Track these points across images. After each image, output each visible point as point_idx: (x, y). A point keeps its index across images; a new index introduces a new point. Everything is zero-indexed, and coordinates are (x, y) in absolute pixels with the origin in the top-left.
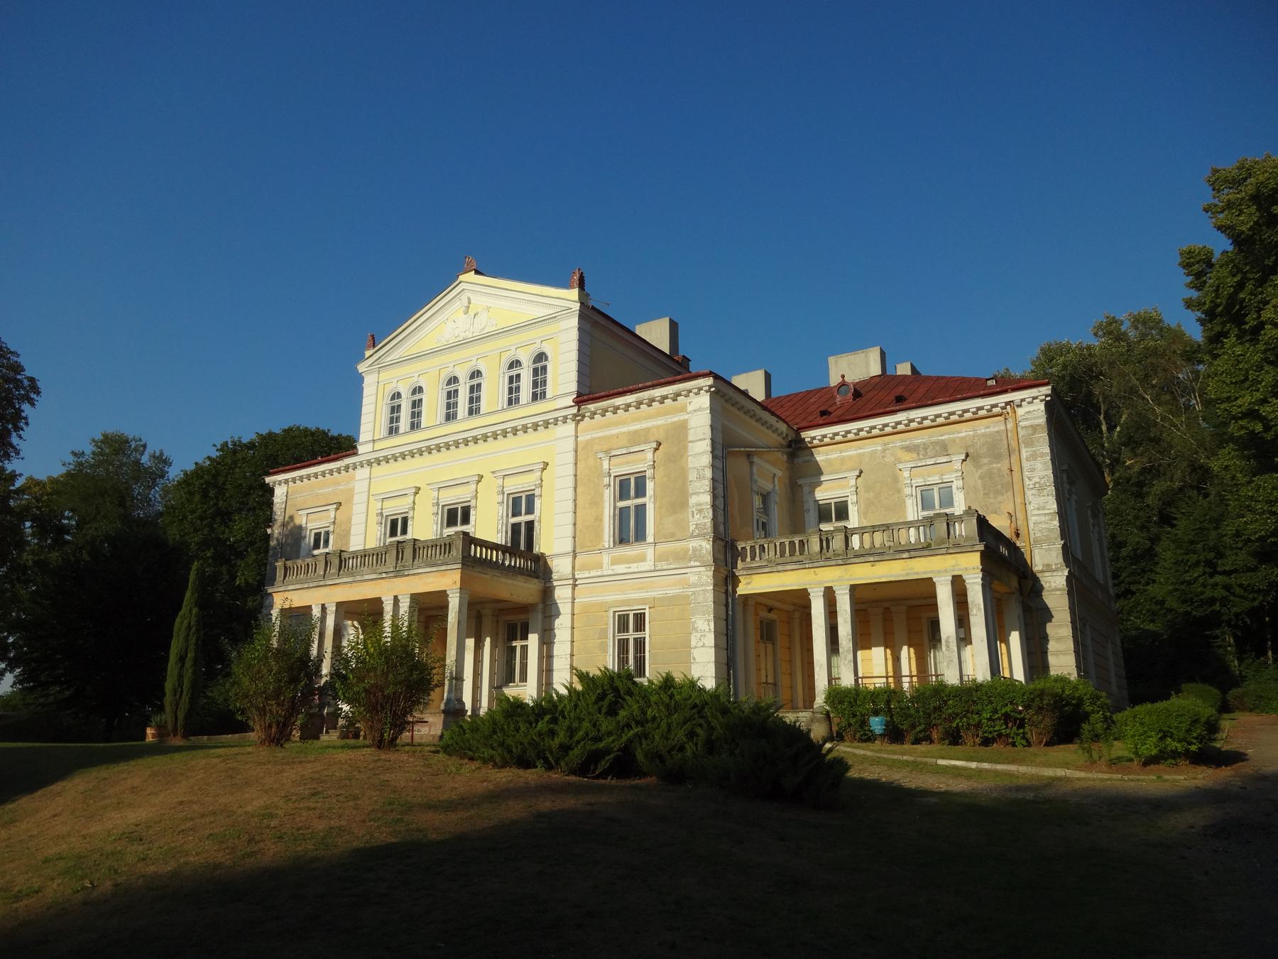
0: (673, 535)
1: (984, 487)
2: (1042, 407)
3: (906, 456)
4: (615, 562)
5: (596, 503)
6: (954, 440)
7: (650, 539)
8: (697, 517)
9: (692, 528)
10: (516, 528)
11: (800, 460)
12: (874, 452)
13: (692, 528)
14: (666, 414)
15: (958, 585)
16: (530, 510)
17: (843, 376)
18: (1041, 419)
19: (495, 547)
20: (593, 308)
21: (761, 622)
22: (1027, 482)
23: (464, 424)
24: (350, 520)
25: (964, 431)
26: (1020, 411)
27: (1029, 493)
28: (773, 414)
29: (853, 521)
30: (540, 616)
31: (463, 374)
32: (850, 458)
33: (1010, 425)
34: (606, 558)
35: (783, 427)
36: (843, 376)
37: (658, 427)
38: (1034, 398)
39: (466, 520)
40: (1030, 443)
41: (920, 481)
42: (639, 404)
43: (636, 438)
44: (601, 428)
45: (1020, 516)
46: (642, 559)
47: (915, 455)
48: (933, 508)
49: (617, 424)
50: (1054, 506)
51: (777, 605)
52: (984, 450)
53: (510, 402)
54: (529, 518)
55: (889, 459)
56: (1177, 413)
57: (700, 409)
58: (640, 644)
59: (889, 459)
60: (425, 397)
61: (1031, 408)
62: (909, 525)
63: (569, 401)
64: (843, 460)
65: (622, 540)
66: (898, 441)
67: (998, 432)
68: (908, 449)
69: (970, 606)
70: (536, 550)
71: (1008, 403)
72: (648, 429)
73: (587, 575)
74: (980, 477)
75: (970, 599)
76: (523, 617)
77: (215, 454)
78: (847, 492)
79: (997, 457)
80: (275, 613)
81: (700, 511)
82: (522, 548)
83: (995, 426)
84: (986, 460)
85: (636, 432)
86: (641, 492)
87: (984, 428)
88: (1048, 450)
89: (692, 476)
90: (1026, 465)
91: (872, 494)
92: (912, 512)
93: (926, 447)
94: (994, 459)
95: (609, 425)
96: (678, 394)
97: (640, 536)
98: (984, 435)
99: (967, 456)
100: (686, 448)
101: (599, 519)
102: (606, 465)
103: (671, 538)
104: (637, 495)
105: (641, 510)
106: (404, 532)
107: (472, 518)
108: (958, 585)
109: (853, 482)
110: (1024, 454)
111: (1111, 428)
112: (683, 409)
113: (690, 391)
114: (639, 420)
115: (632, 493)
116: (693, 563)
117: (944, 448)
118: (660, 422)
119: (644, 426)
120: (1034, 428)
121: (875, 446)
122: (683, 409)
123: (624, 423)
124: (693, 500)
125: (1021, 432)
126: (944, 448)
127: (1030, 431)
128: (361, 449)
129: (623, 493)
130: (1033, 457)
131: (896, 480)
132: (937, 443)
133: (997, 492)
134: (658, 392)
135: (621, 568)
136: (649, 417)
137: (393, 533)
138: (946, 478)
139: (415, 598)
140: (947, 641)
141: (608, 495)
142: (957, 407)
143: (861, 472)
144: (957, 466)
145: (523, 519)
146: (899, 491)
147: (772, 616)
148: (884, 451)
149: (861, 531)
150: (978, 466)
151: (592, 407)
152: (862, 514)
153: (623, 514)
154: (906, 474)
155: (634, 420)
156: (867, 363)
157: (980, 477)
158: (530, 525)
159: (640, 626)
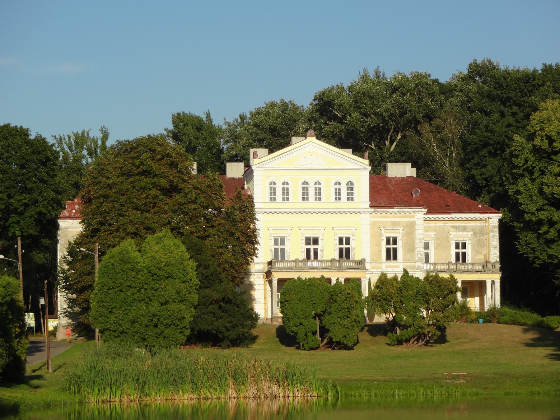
0: (409, 260)
2: (498, 220)
4: (387, 267)
5: (379, 245)
6: (468, 226)
9: (417, 259)
10: (341, 250)
12: (441, 226)
13: (417, 259)
14: (407, 217)
15: (493, 282)
16: (348, 242)
18: (497, 224)
23: (312, 203)
25: (472, 224)
26: (491, 220)
32: (432, 227)
33: (487, 224)
37: (403, 221)
40: (493, 232)
43: (394, 224)
44: (379, 217)
45: (487, 255)
46: (399, 267)
49: (387, 217)
50: (498, 254)
52: (478, 232)
54: (347, 246)
56: (445, 156)
57: (420, 218)
59: (446, 229)
60: (290, 187)
61: (494, 220)
63: (367, 205)
65: (388, 258)
66: (449, 224)
68: (453, 227)
72: (399, 222)
73: (375, 270)
74: (477, 241)
78: (430, 239)
80: (58, 257)
81: (420, 254)
83: (482, 224)
84: (478, 235)
85: (394, 222)
87: (479, 224)
88: (498, 235)
89: (417, 241)
90: (491, 239)
93: (459, 227)
94: (480, 234)
95: (383, 217)
97: (395, 258)
101: (380, 251)
102: (383, 232)
103: (408, 261)
105: (395, 250)
108: (493, 282)
109: (433, 236)
111: (392, 142)
114: (396, 217)
117: (465, 229)
120: (495, 227)
121: (441, 224)
122: (413, 217)
123: (390, 217)
124: (417, 250)
129: (388, 242)
130: (494, 236)
131: (448, 237)
133: (481, 247)
134: (406, 210)
136: (399, 217)
138: (465, 239)
142: (472, 215)
144: (470, 236)
145: (344, 246)
146: (449, 241)
150: (476, 237)
151: (379, 210)
152: (436, 248)
153: (388, 250)
155: (394, 217)
156: (405, 169)
157: (477, 241)
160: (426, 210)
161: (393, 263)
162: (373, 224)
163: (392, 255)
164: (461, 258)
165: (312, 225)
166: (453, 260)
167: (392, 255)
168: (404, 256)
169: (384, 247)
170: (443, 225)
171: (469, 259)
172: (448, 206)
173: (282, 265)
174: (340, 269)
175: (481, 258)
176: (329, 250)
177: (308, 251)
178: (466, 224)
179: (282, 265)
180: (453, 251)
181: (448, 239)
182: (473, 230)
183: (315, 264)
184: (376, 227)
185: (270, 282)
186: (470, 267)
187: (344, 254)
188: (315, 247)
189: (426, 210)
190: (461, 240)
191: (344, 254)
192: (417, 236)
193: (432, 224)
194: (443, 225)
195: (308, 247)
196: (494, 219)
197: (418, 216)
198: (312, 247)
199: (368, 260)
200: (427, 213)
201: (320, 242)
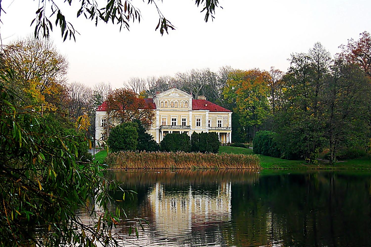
3: (217, 117)
25: (223, 115)
31: (174, 102)
65: (197, 125)
83: (226, 115)
86: (200, 121)
89: (206, 120)
97: (199, 125)
105: (200, 123)
112: (206, 113)
121: (214, 115)
124: (206, 123)
126: (221, 116)
139: (184, 132)
141: (196, 120)
153: (197, 123)
160: (209, 111)
161: (198, 127)
162: (192, 114)
163: (198, 124)
164: (220, 126)
165: (174, 115)
166: (217, 126)
167: (198, 124)
169: (196, 122)
171: (222, 126)
172: (216, 109)
173: (165, 127)
174: (183, 129)
175: (226, 126)
176: (179, 123)
177: (173, 123)
178: (221, 115)
179: (165, 127)
180: (217, 123)
181: (216, 120)
183: (175, 127)
184: (194, 116)
186: (222, 129)
187: (184, 124)
188: (175, 121)
189: (209, 111)
190: (220, 120)
191: (184, 124)
193: (211, 115)
195: (173, 121)
196: (230, 113)
197: (207, 112)
198: (174, 121)
199: (191, 126)
200: (210, 111)
201: (176, 120)
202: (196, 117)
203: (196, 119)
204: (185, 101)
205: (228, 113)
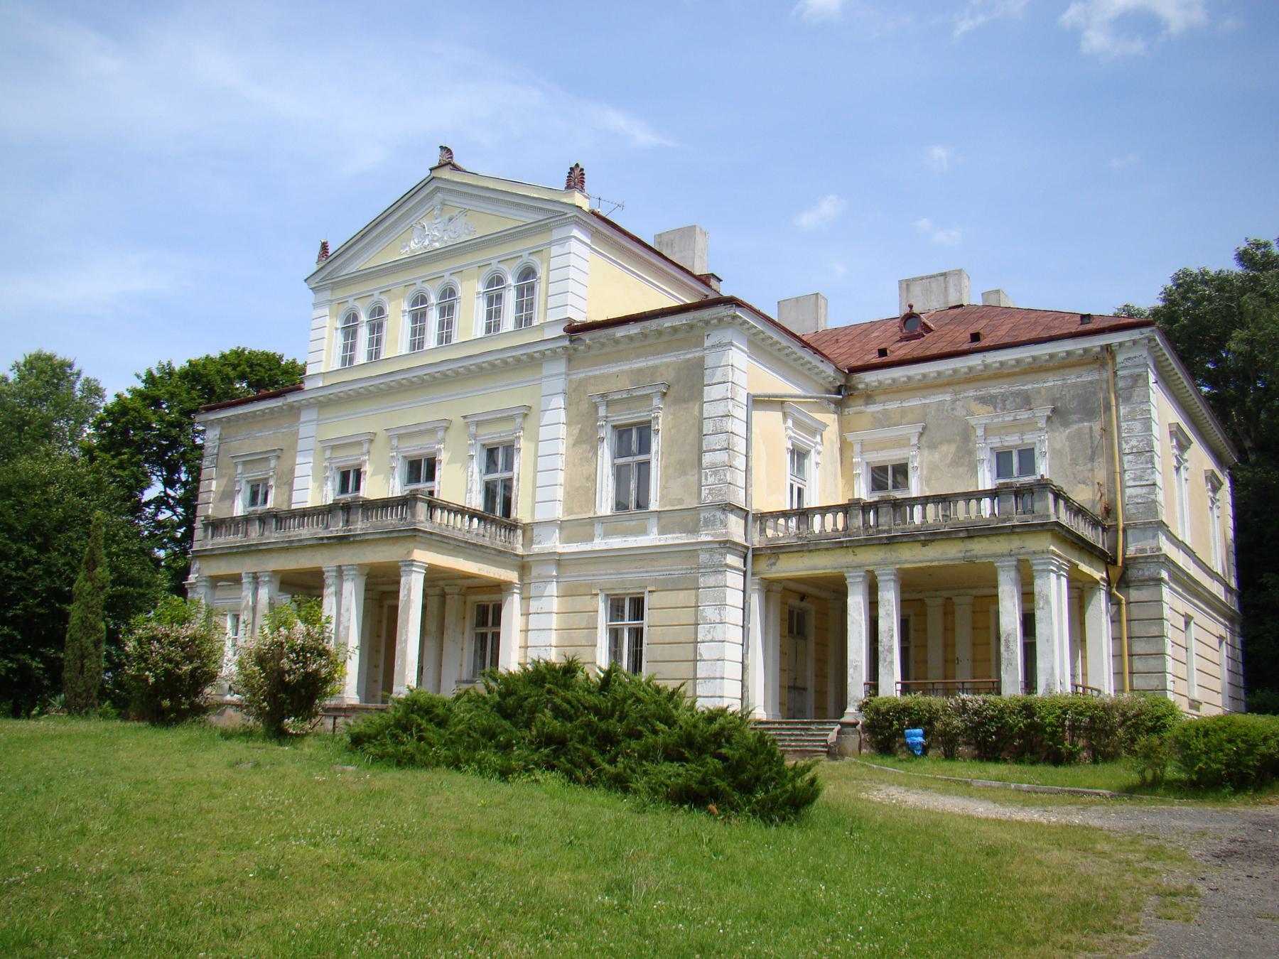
0: (681, 501)
1: (1072, 449)
6: (1038, 391)
7: (654, 506)
8: (711, 480)
11: (852, 410)
13: (704, 493)
17: (911, 307)
19: (461, 511)
20: (593, 213)
21: (791, 613)
22: (1124, 446)
24: (292, 471)
25: (1051, 382)
27: (1126, 458)
28: (816, 351)
29: (915, 488)
30: (516, 598)
32: (912, 409)
34: (598, 529)
35: (829, 370)
36: (911, 307)
37: (667, 365)
38: (1135, 342)
39: (431, 476)
41: (996, 442)
42: (644, 336)
47: (991, 408)
48: (1010, 474)
51: (811, 590)
53: (488, 330)
54: (506, 475)
55: (960, 412)
58: (637, 634)
59: (960, 412)
62: (979, 495)
64: (903, 412)
65: (621, 505)
67: (1091, 382)
68: (983, 400)
69: (1037, 597)
70: (513, 515)
71: (1107, 348)
72: (656, 367)
75: (1037, 589)
76: (494, 597)
77: (140, 386)
79: (1090, 414)
82: (499, 512)
83: (1087, 376)
84: (1075, 417)
85: (640, 371)
86: (645, 447)
89: (708, 427)
91: (937, 456)
92: (986, 480)
96: (691, 327)
98: (1075, 385)
99: (1053, 411)
100: (702, 392)
101: (592, 478)
104: (640, 453)
106: (357, 488)
107: (437, 474)
110: (1122, 411)
113: (707, 323)
115: (634, 447)
116: (704, 538)
117: (1026, 401)
118: (669, 358)
119: (651, 363)
124: (707, 459)
125: (1121, 384)
127: (1129, 382)
128: (308, 385)
132: (1017, 394)
135: (617, 542)
137: (344, 489)
138: (1029, 438)
140: (1007, 641)
143: (924, 428)
145: (499, 476)
147: (804, 604)
148: (954, 402)
149: (924, 501)
152: (926, 481)
154: (980, 432)
156: (946, 288)
158: (508, 485)
159: (638, 612)
168: (664, 488)
170: (948, 398)
182: (1053, 401)
185: (381, 607)
192: (708, 410)
194: (948, 398)
202: (602, 411)
203: (606, 432)
204: (517, 264)
205: (1097, 342)
